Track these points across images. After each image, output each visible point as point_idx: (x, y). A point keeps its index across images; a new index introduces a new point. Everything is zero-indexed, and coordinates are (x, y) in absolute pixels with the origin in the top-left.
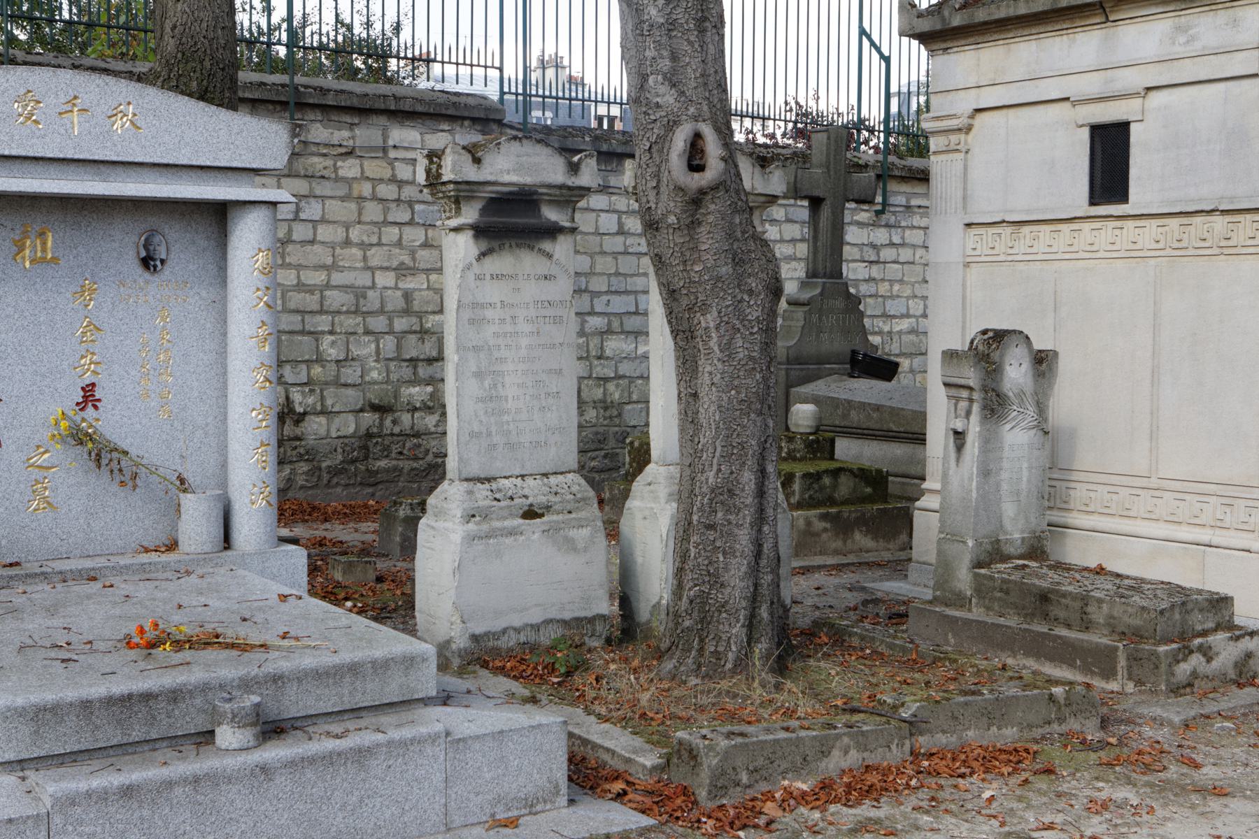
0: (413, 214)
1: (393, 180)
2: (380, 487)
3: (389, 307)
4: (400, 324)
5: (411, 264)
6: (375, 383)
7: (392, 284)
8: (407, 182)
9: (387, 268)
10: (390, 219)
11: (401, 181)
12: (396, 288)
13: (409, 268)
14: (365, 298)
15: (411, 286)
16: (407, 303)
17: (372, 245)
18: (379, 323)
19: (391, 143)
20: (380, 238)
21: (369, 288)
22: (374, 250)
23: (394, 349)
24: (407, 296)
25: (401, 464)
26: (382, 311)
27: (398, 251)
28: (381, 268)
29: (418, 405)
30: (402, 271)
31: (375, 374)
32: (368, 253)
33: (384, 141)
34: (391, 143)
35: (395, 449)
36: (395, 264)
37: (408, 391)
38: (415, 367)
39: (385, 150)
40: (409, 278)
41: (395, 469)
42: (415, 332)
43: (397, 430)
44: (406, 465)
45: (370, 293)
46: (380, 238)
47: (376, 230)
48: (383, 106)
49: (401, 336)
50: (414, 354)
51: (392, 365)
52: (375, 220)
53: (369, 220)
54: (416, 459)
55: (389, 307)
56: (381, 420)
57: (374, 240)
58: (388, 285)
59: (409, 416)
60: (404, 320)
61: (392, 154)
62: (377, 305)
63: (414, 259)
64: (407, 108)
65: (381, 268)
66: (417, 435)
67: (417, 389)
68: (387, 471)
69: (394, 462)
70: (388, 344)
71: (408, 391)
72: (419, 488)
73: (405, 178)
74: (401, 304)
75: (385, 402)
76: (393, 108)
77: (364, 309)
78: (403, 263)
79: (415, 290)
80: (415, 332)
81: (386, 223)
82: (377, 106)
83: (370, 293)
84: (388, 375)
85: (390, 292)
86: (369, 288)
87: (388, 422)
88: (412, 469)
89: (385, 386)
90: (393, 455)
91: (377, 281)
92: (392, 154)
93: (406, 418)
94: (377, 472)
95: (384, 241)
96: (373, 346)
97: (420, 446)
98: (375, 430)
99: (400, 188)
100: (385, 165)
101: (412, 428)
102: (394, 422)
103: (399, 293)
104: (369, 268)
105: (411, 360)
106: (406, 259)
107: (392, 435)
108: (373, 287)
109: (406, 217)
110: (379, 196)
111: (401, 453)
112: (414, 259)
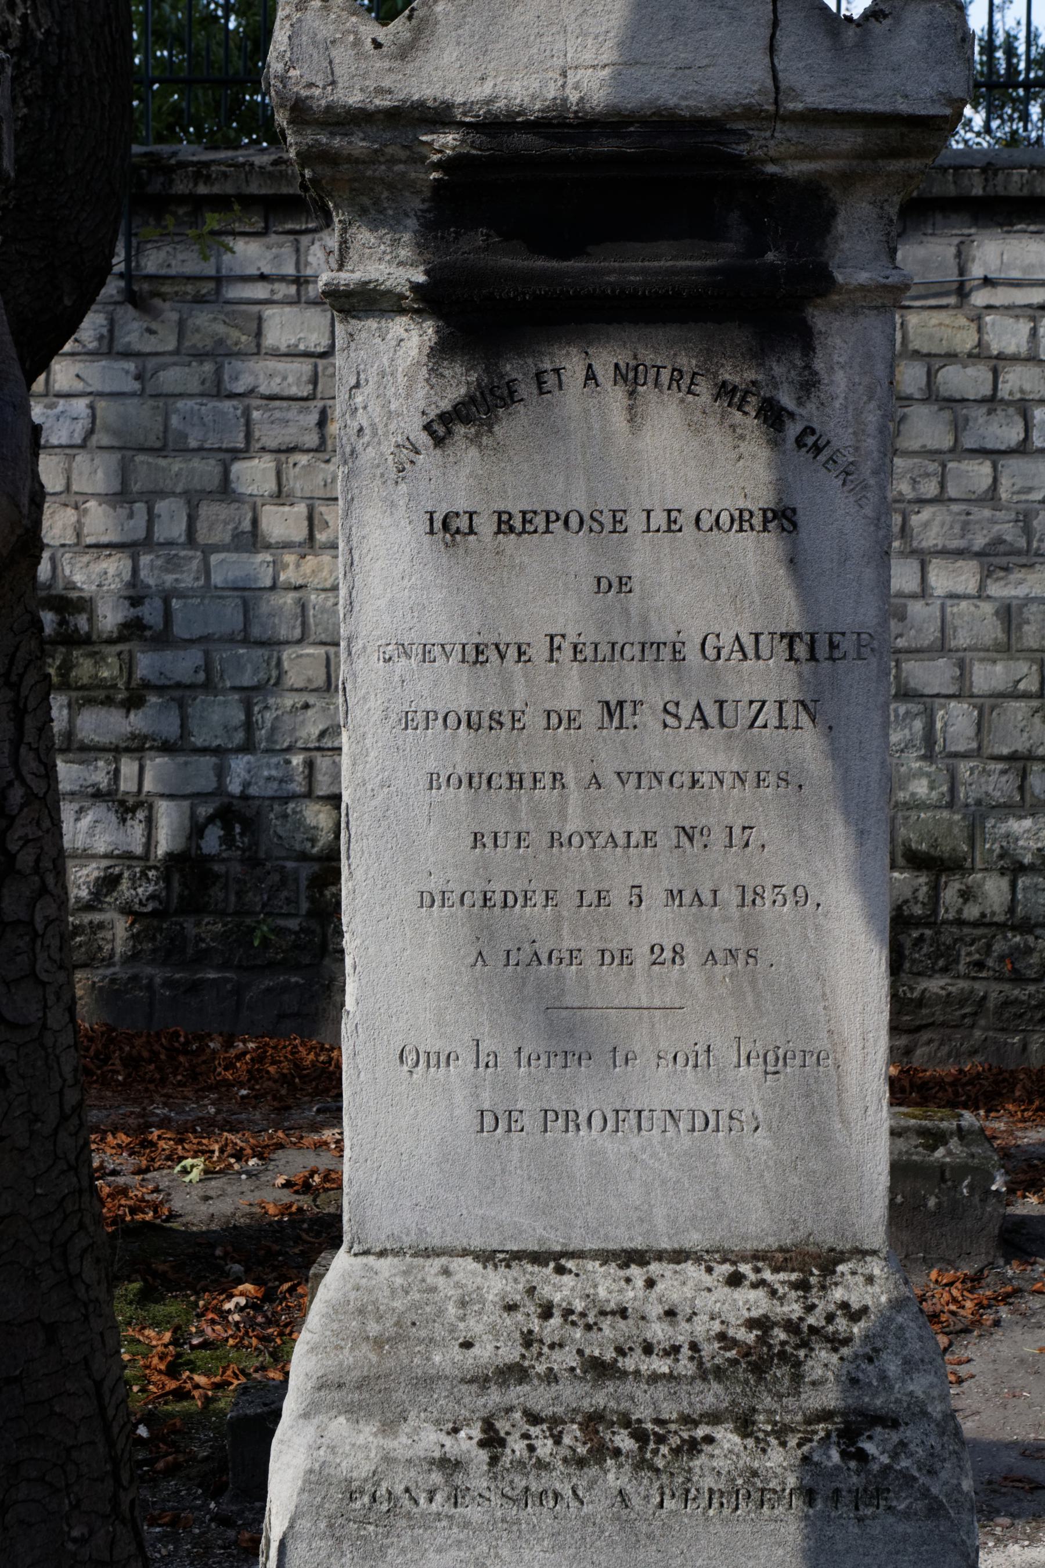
0: (1027, 430)
1: (979, 354)
2: (925, 1036)
3: (962, 639)
4: (988, 676)
5: (1022, 543)
6: (921, 806)
7: (972, 587)
8: (1015, 358)
9: (960, 553)
10: (969, 442)
11: (1000, 357)
12: (981, 595)
13: (1018, 553)
14: (902, 618)
15: (1021, 591)
16: (1008, 631)
17: (922, 502)
18: (932, 675)
19: (977, 271)
20: (942, 485)
21: (913, 596)
22: (927, 513)
23: (971, 731)
24: (1009, 615)
25: (980, 989)
26: (941, 648)
27: (987, 513)
28: (943, 552)
29: (1027, 860)
30: (995, 560)
31: (920, 788)
32: (915, 520)
33: (962, 271)
34: (977, 271)
35: (967, 955)
36: (980, 542)
37: (1003, 828)
38: (1024, 775)
39: (962, 292)
40: (1016, 575)
41: (963, 1000)
42: (1026, 696)
43: (972, 912)
44: (995, 992)
45: (916, 608)
46: (942, 485)
47: (933, 467)
48: (951, 191)
49: (987, 707)
50: (1020, 744)
51: (964, 768)
52: (933, 444)
53: (915, 445)
54: (1018, 978)
55: (962, 639)
56: (935, 889)
57: (930, 489)
58: (960, 589)
59: (1004, 883)
60: (999, 668)
61: (980, 298)
62: (931, 634)
63: (1028, 531)
64: (1014, 190)
65: (943, 552)
66: (1025, 926)
67: (1027, 823)
68: (948, 1000)
69: (962, 984)
70: (957, 722)
71: (1003, 828)
72: (1025, 1047)
73: (1011, 349)
74: (991, 630)
75: (945, 848)
76: (978, 191)
77: (901, 643)
78: (999, 541)
79: (1028, 600)
80: (1026, 696)
81: (958, 451)
82: (937, 190)
83: (916, 608)
84: (953, 790)
85: (964, 604)
86: (913, 596)
87: (950, 894)
88: (1007, 1003)
89: (945, 814)
90: (962, 968)
91: (933, 579)
92: (980, 298)
93: (994, 890)
94: (920, 1002)
95: (952, 492)
96: (918, 725)
97: (1029, 951)
98: (918, 910)
99: (995, 373)
100: (963, 321)
101: (1011, 910)
102: (966, 895)
103: (987, 608)
104: (914, 552)
105: (1013, 757)
106: (1010, 532)
107: (960, 922)
108: (924, 592)
109: (1013, 434)
110: (944, 392)
111: (980, 965)
112: (1028, 531)
